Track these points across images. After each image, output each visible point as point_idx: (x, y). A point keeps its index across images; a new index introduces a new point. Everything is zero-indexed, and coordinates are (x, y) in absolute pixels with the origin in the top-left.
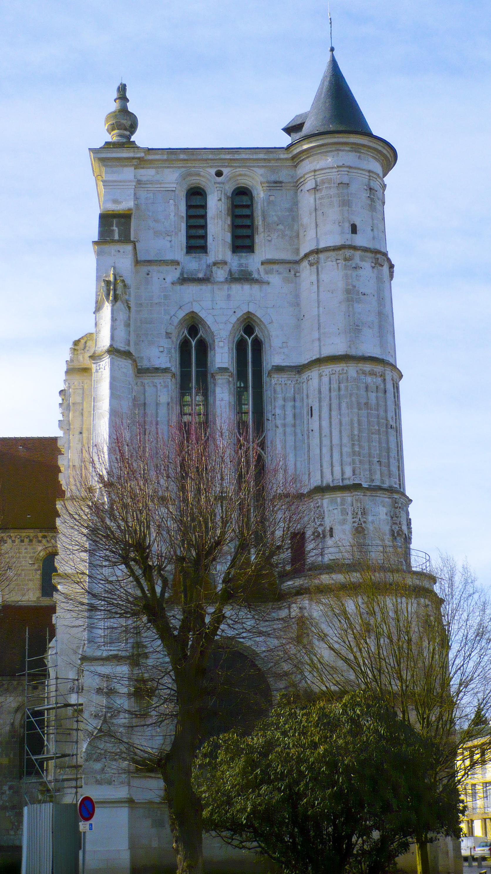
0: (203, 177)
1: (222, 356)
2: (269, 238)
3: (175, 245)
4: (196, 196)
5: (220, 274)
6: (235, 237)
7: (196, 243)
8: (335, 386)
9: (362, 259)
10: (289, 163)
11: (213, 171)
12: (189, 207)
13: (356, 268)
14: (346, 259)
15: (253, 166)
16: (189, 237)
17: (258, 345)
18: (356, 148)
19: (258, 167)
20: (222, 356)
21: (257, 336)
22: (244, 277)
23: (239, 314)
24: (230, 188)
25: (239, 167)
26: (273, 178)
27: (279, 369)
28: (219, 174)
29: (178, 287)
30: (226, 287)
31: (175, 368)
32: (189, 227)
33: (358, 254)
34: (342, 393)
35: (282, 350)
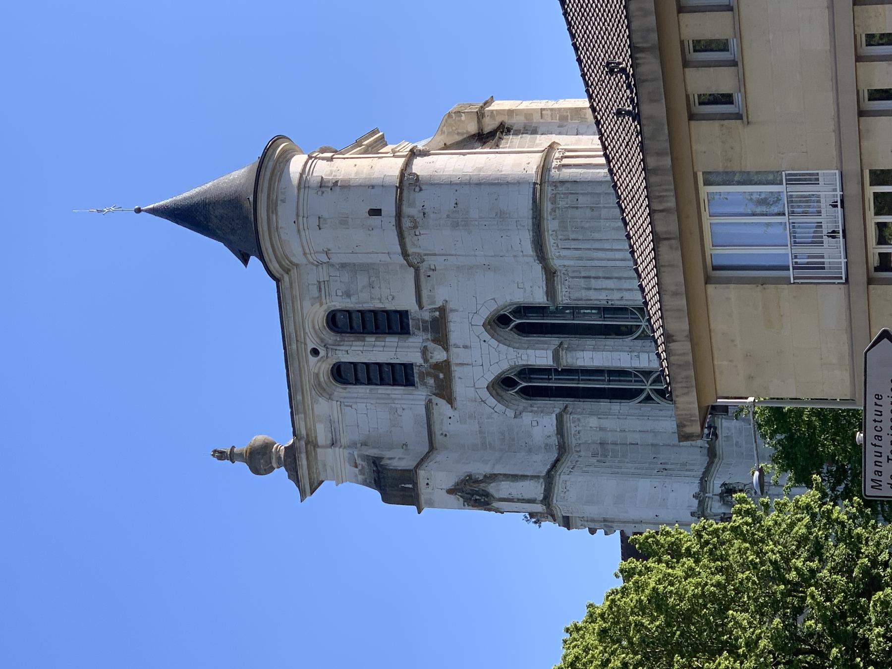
0: (320, 368)
1: (539, 354)
2: (390, 298)
3: (409, 402)
4: (342, 374)
5: (439, 355)
6: (391, 332)
7: (399, 375)
8: (573, 245)
9: (412, 205)
10: (294, 272)
11: (312, 360)
12: (357, 382)
13: (424, 214)
14: (415, 227)
15: (302, 314)
16: (395, 383)
17: (522, 310)
18: (272, 207)
19: (302, 308)
20: (539, 354)
21: (510, 313)
22: (438, 326)
23: (487, 336)
24: (330, 337)
25: (304, 329)
26: (314, 292)
27: (551, 292)
28: (315, 352)
29: (458, 403)
30: (453, 350)
31: (558, 404)
32: (382, 382)
33: (406, 210)
34: (581, 237)
35: (528, 289)
